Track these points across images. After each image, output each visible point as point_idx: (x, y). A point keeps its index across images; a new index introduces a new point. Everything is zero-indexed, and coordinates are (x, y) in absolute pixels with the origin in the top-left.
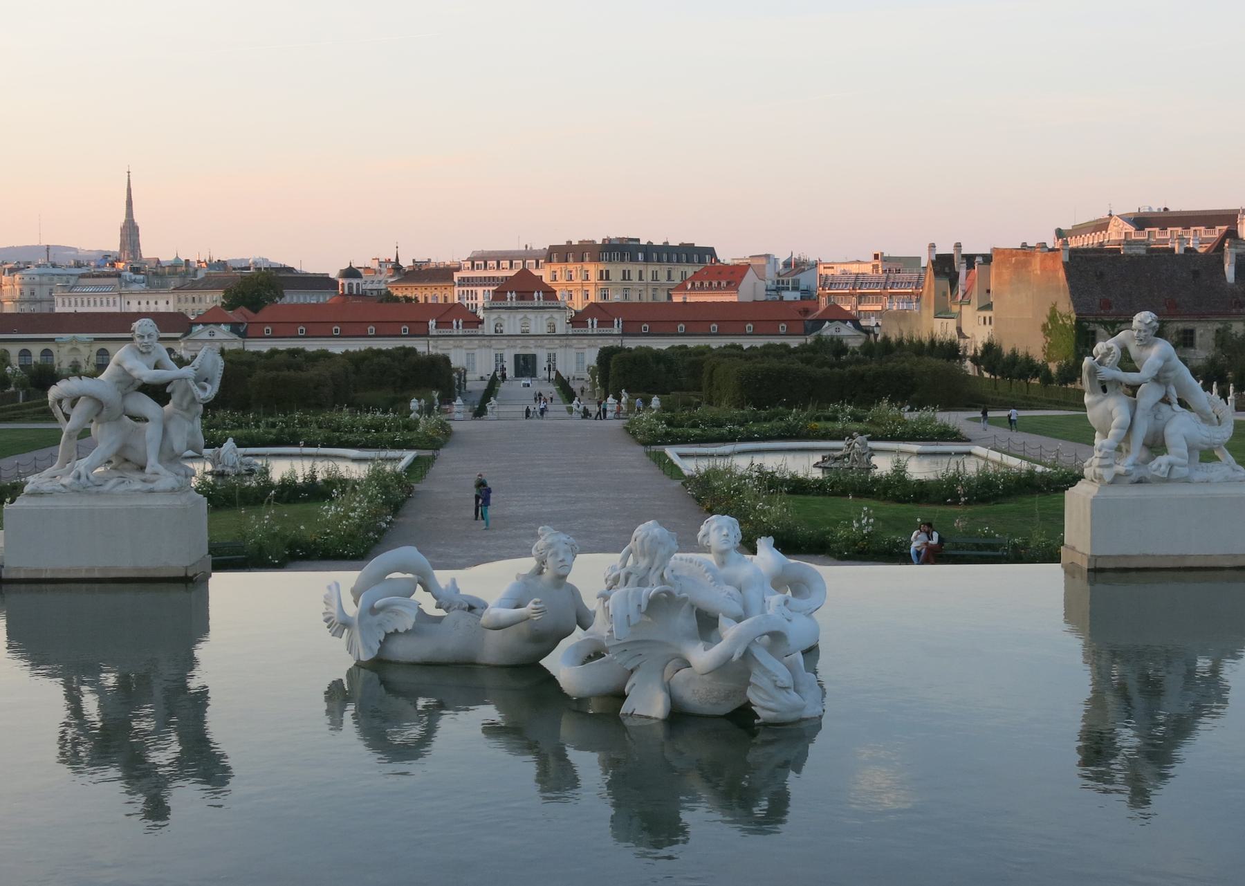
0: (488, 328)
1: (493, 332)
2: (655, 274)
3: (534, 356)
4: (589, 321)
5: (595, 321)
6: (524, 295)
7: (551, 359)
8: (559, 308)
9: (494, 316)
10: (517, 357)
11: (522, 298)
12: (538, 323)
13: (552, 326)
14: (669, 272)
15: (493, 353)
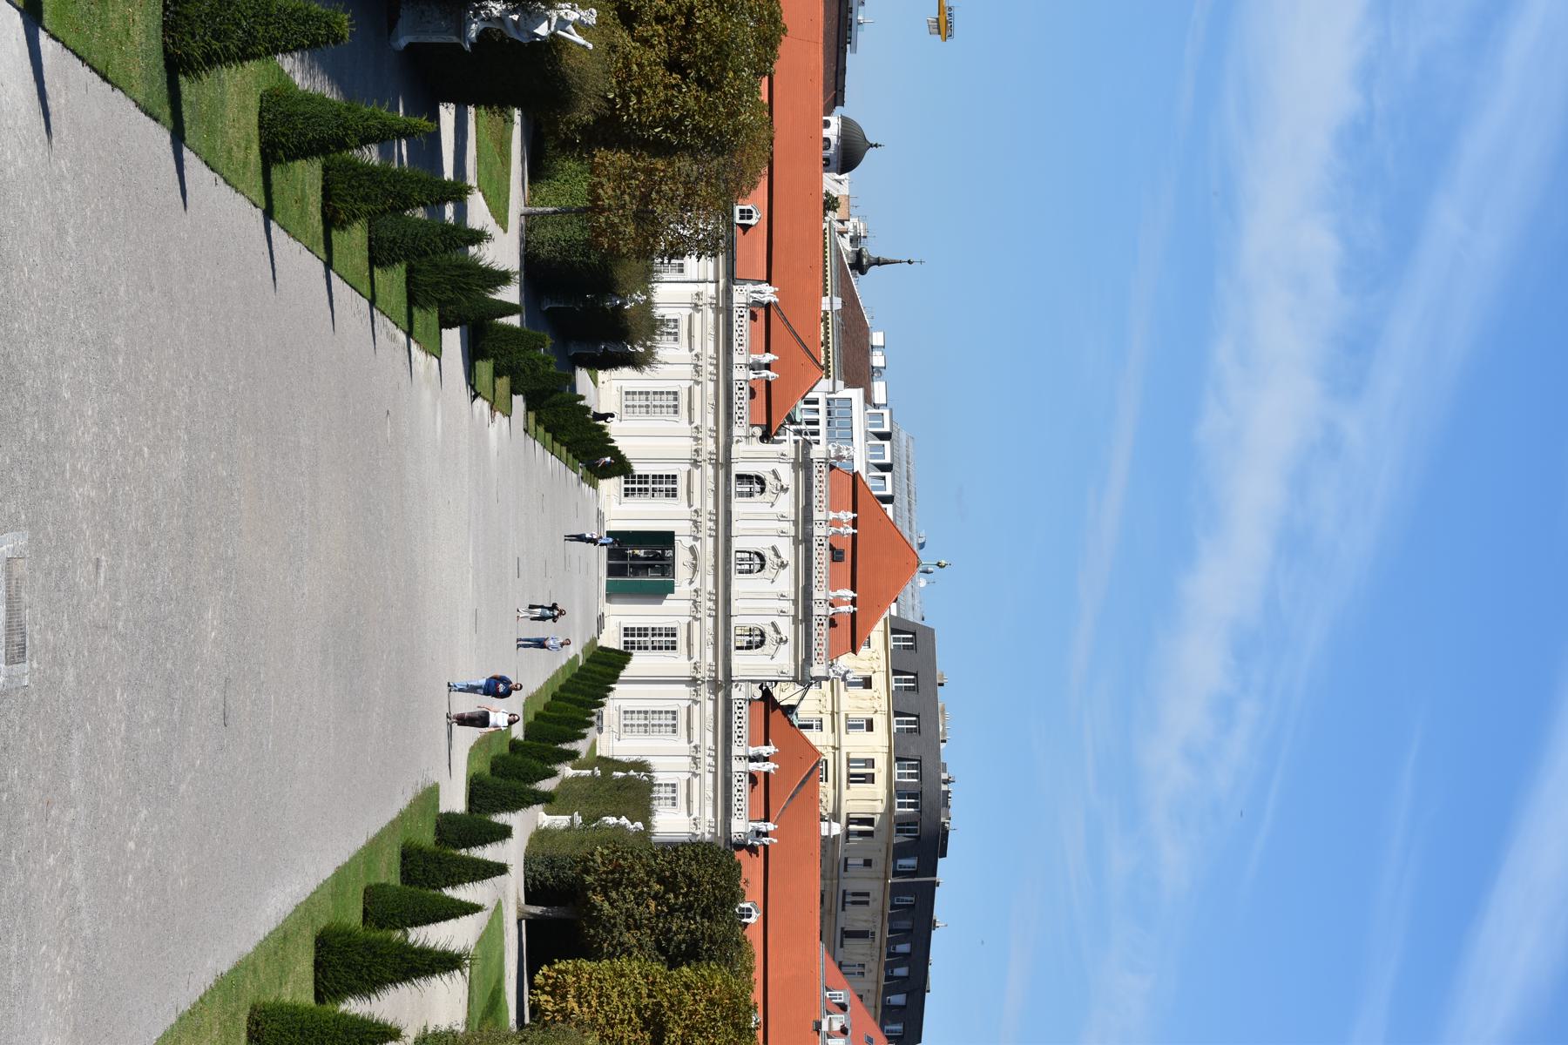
0: (750, 454)
1: (737, 469)
2: (861, 898)
3: (669, 588)
4: (770, 750)
5: (769, 767)
6: (847, 556)
7: (665, 640)
8: (808, 661)
9: (787, 474)
10: (667, 539)
11: (836, 555)
12: (763, 599)
13: (756, 641)
14: (862, 934)
15: (681, 470)
